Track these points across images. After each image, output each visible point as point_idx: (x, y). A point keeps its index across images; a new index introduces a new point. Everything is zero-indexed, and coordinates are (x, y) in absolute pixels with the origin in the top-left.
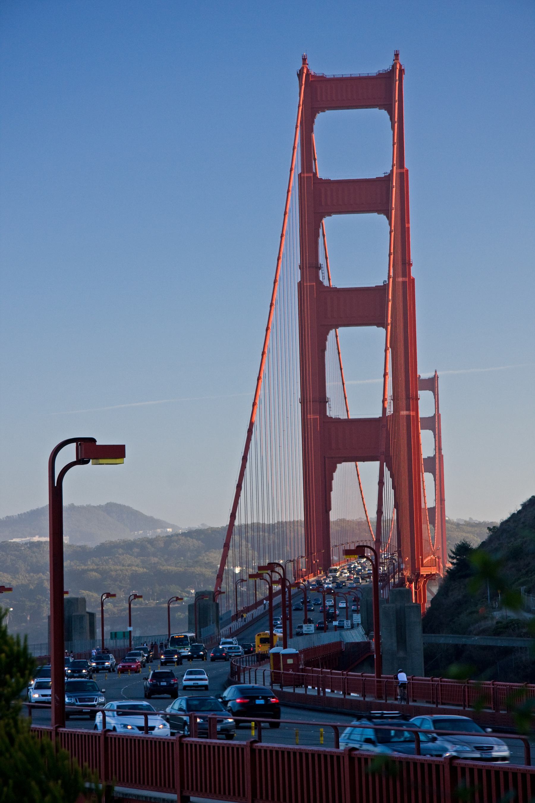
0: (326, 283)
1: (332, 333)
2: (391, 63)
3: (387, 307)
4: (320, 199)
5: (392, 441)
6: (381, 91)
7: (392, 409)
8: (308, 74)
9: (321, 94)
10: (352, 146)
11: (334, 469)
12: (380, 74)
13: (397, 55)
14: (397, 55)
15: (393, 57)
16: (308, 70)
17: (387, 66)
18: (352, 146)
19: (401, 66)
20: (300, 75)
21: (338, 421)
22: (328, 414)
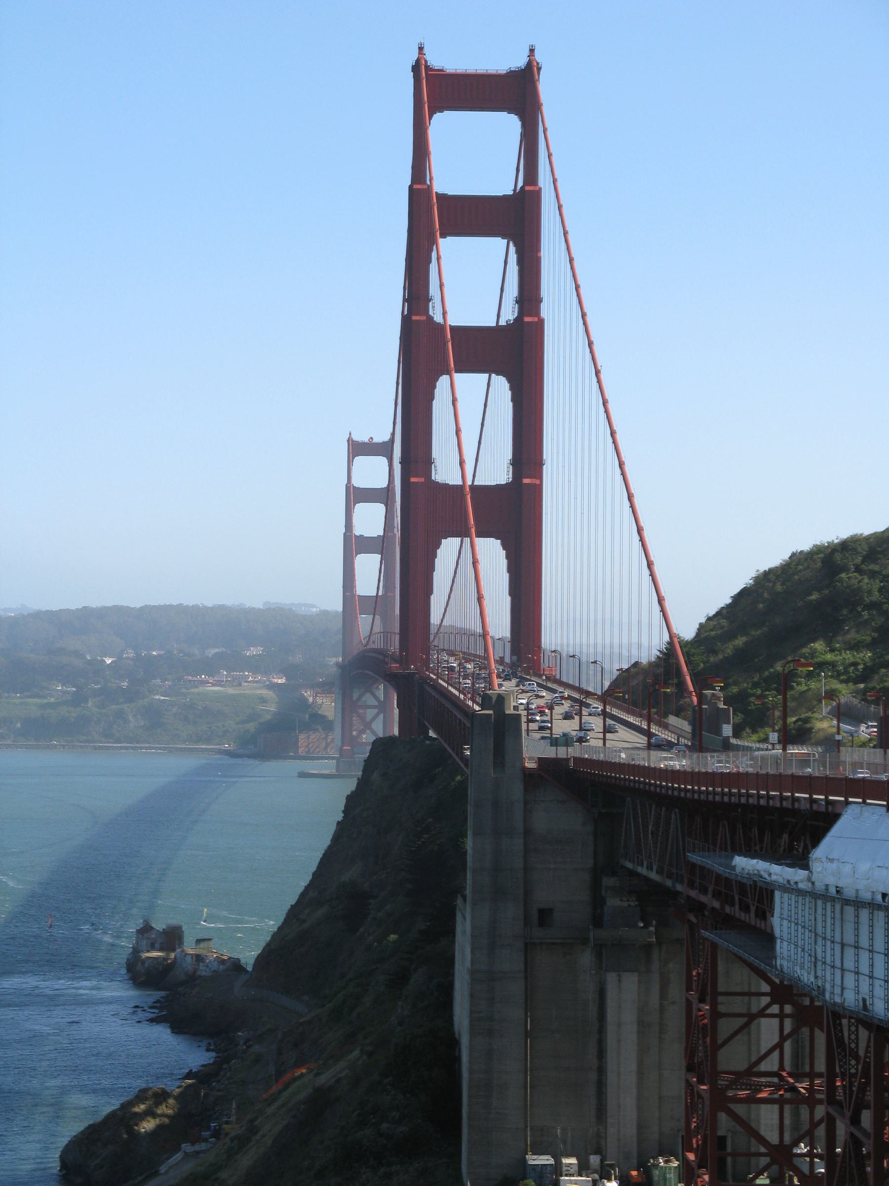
0: (438, 318)
1: (443, 382)
2: (526, 60)
3: (513, 352)
4: (435, 217)
5: (512, 513)
6: (514, 92)
7: (511, 476)
8: (427, 68)
9: (441, 91)
10: (476, 154)
11: (438, 545)
12: (511, 71)
13: (532, 51)
14: (532, 51)
15: (527, 53)
16: (426, 62)
17: (519, 62)
18: (476, 154)
19: (538, 63)
20: (416, 68)
21: (446, 487)
22: (433, 478)
